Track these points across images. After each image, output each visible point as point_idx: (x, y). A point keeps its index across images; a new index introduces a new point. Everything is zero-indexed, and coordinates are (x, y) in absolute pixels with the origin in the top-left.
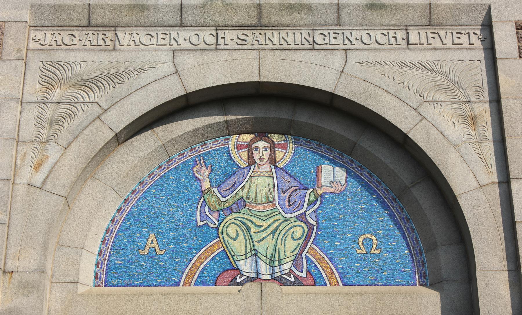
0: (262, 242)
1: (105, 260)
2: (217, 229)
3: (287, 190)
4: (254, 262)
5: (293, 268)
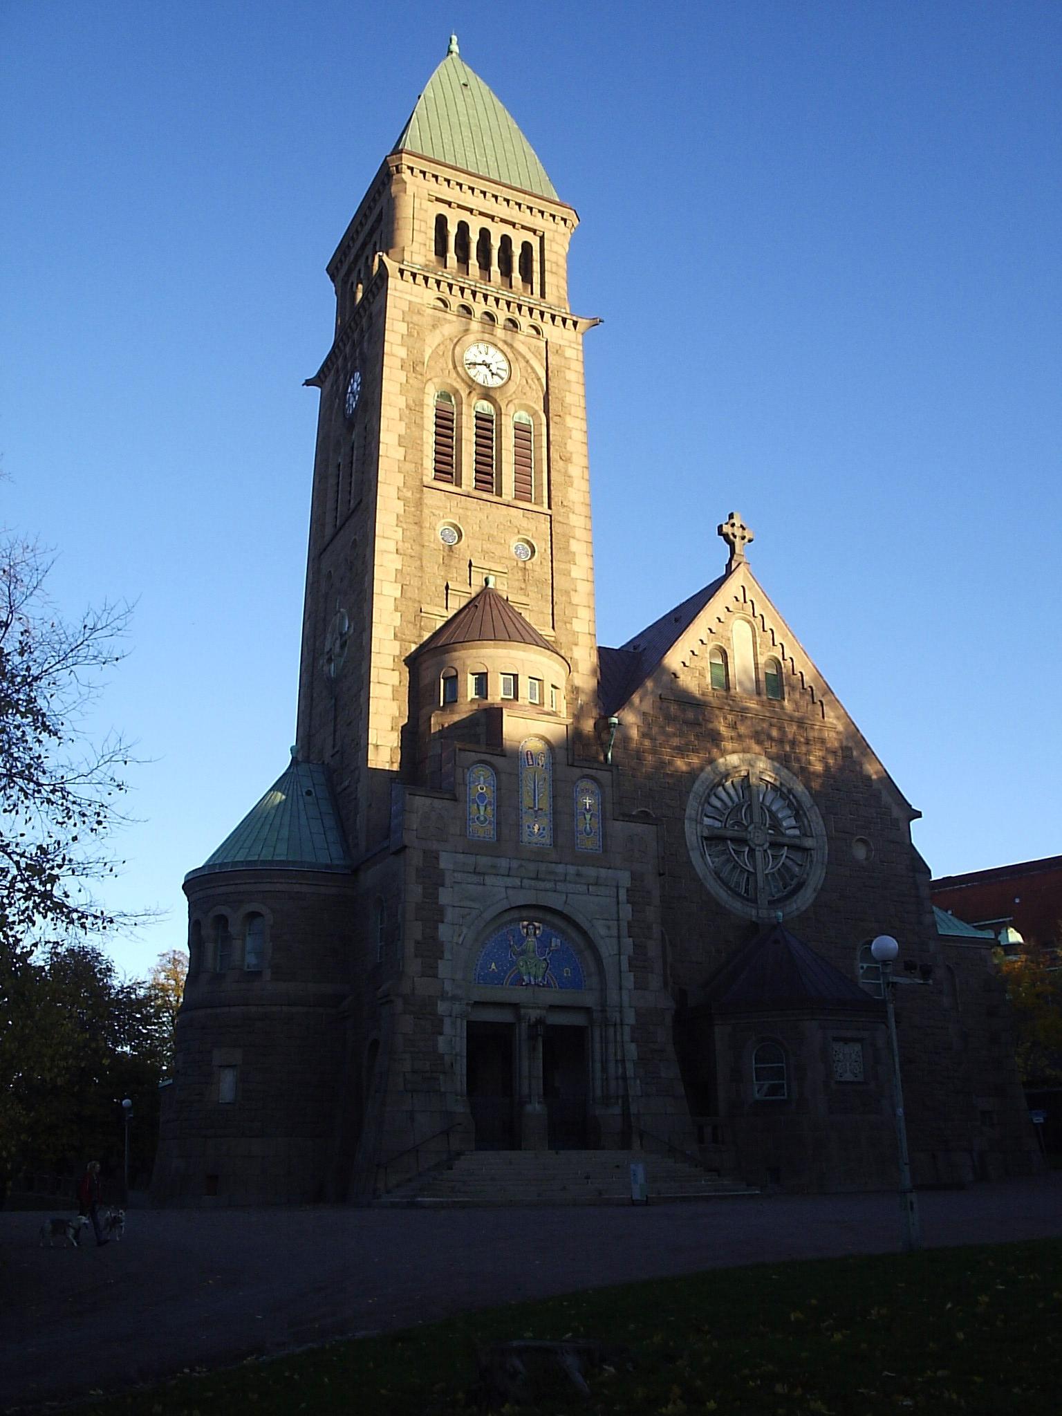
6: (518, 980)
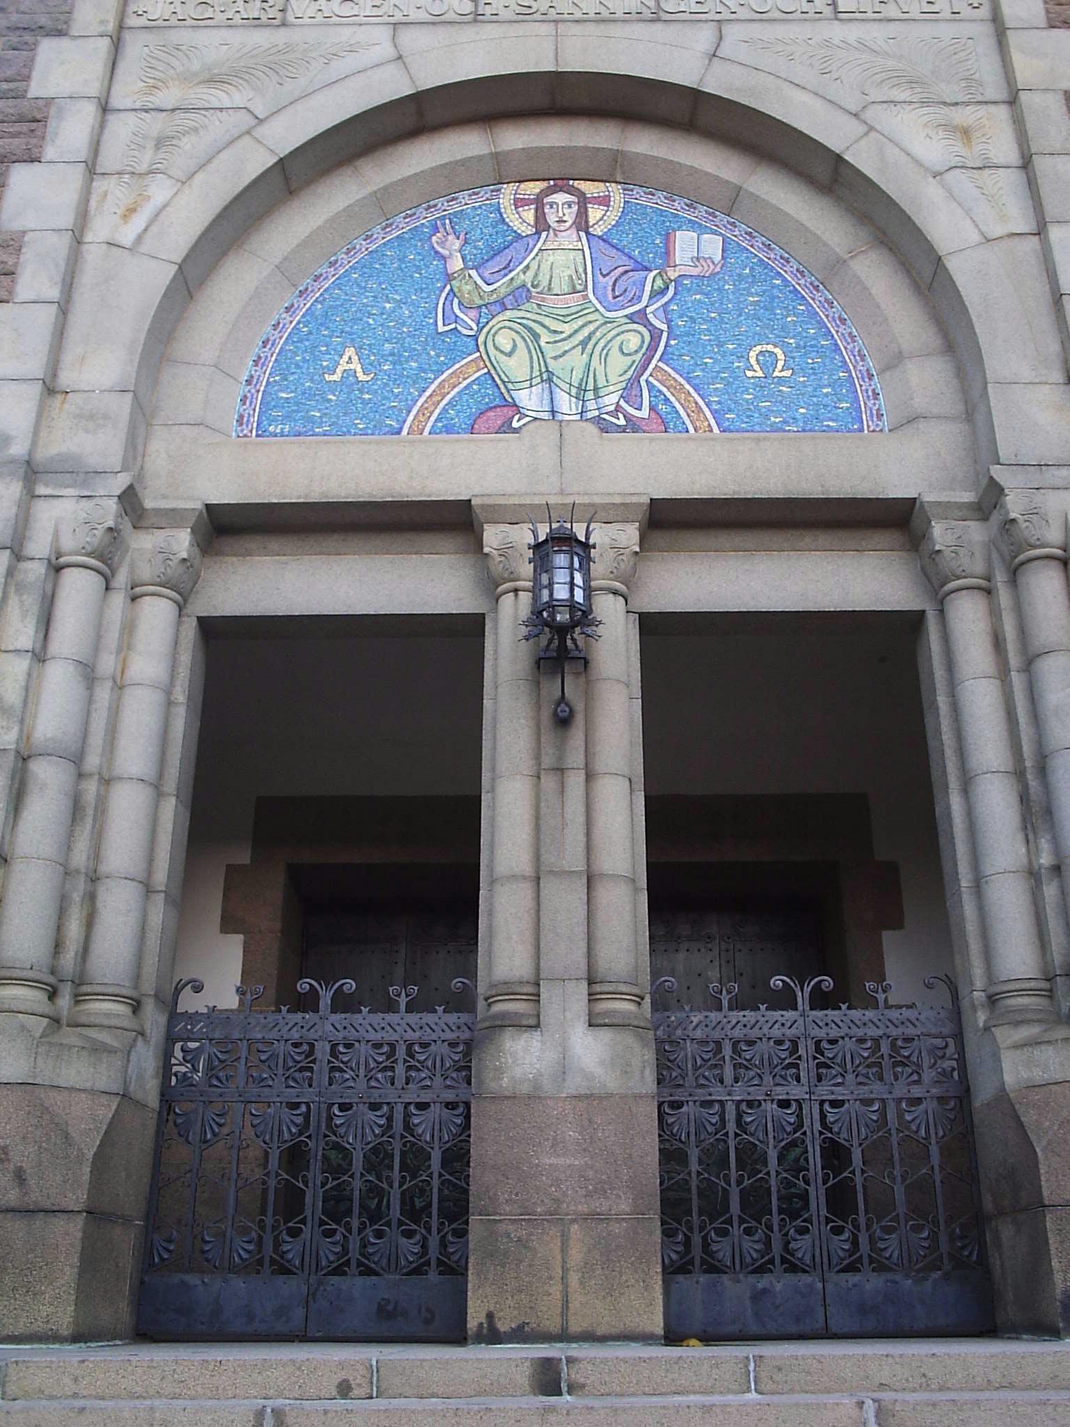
2: (476, 338)
4: (547, 393)
5: (622, 402)
6: (496, 411)
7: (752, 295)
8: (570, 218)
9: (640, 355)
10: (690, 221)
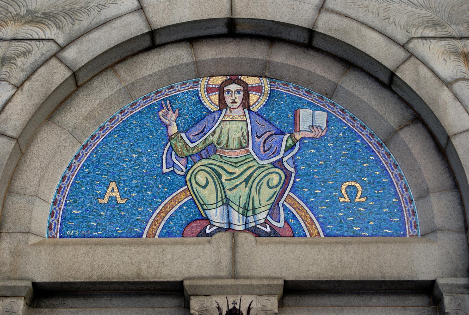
0: (234, 191)
1: (60, 209)
2: (185, 176)
3: (262, 135)
4: (226, 211)
5: (269, 218)
7: (343, 149)
8: (239, 101)
9: (279, 188)
10: (308, 102)
